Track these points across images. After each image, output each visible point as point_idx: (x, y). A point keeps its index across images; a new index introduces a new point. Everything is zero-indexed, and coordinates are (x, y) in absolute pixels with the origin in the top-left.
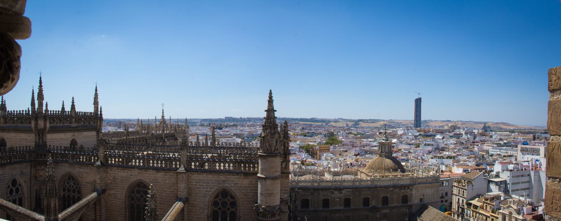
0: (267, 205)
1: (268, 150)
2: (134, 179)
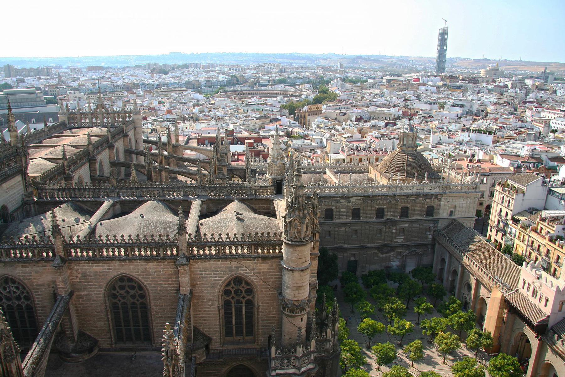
0: (296, 299)
1: (296, 238)
2: (113, 274)
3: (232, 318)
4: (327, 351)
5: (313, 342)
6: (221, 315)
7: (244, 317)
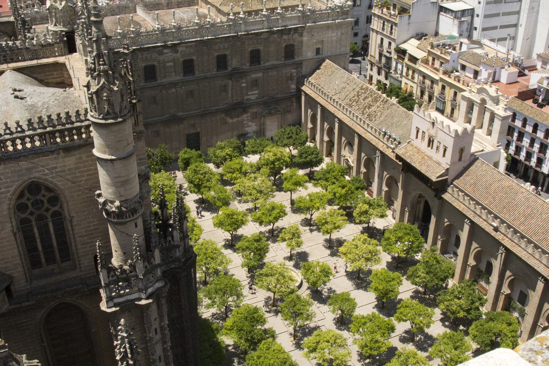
0: (123, 199)
3: (36, 242)
4: (178, 260)
5: (157, 253)
6: (19, 241)
7: (53, 237)
